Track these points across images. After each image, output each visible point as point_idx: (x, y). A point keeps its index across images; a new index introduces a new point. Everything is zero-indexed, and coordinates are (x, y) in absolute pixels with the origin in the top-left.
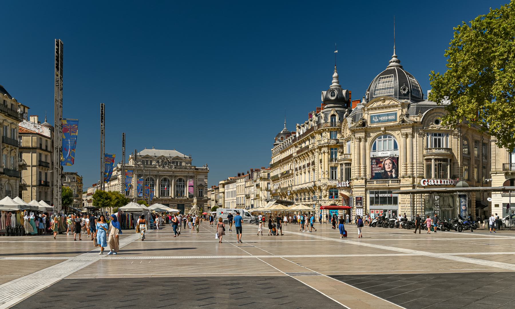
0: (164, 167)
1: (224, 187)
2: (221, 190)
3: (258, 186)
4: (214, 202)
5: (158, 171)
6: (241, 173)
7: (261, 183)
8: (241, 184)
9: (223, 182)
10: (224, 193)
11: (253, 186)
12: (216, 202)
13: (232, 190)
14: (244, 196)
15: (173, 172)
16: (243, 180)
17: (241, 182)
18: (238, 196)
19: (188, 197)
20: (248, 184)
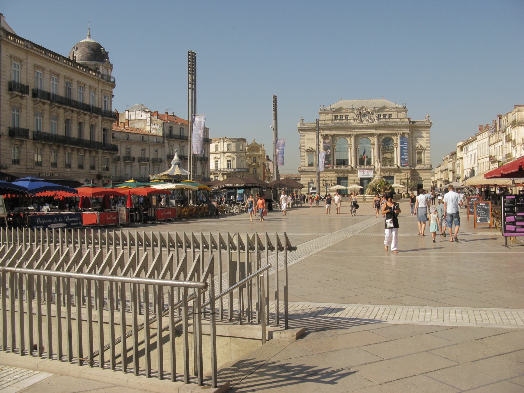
0: (361, 121)
1: (462, 150)
2: (459, 155)
3: (508, 139)
4: (452, 172)
5: (354, 128)
6: (485, 126)
7: (513, 132)
8: (484, 141)
9: (461, 143)
10: (462, 158)
11: (501, 140)
12: (454, 173)
13: (471, 153)
14: (488, 159)
15: (376, 128)
16: (486, 134)
17: (484, 139)
18: (480, 161)
19: (399, 165)
20: (493, 139)
